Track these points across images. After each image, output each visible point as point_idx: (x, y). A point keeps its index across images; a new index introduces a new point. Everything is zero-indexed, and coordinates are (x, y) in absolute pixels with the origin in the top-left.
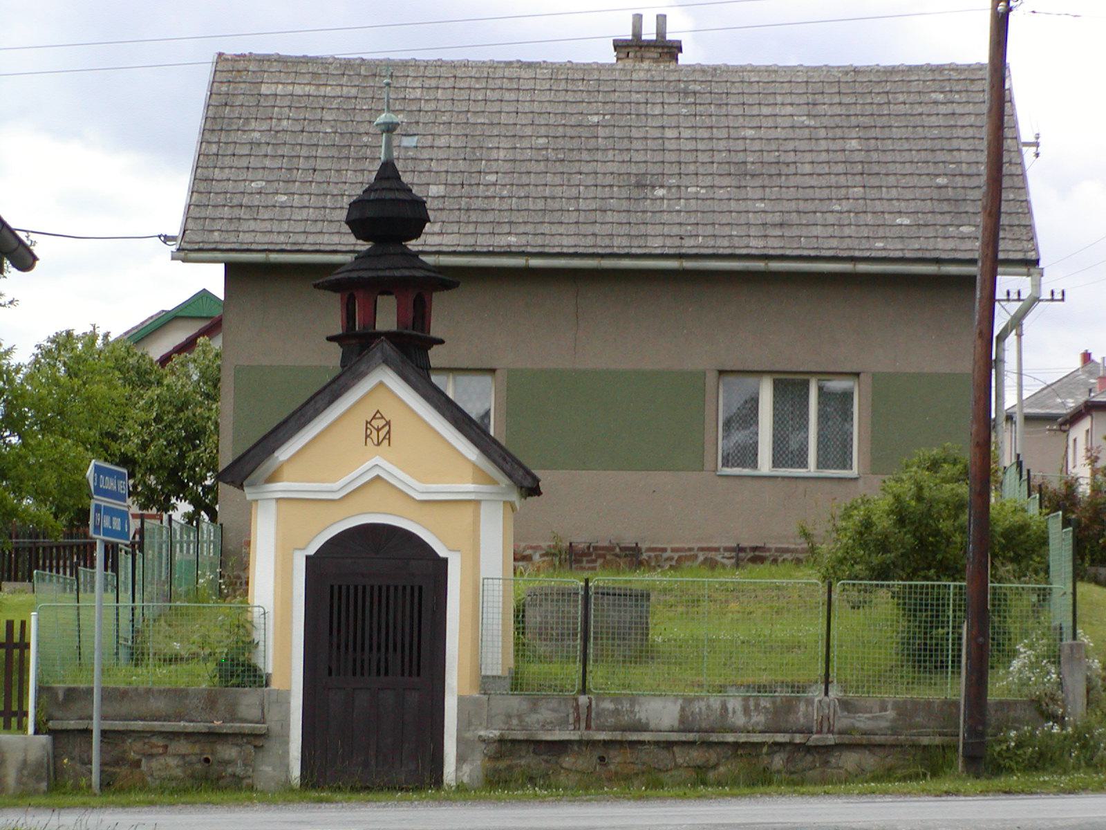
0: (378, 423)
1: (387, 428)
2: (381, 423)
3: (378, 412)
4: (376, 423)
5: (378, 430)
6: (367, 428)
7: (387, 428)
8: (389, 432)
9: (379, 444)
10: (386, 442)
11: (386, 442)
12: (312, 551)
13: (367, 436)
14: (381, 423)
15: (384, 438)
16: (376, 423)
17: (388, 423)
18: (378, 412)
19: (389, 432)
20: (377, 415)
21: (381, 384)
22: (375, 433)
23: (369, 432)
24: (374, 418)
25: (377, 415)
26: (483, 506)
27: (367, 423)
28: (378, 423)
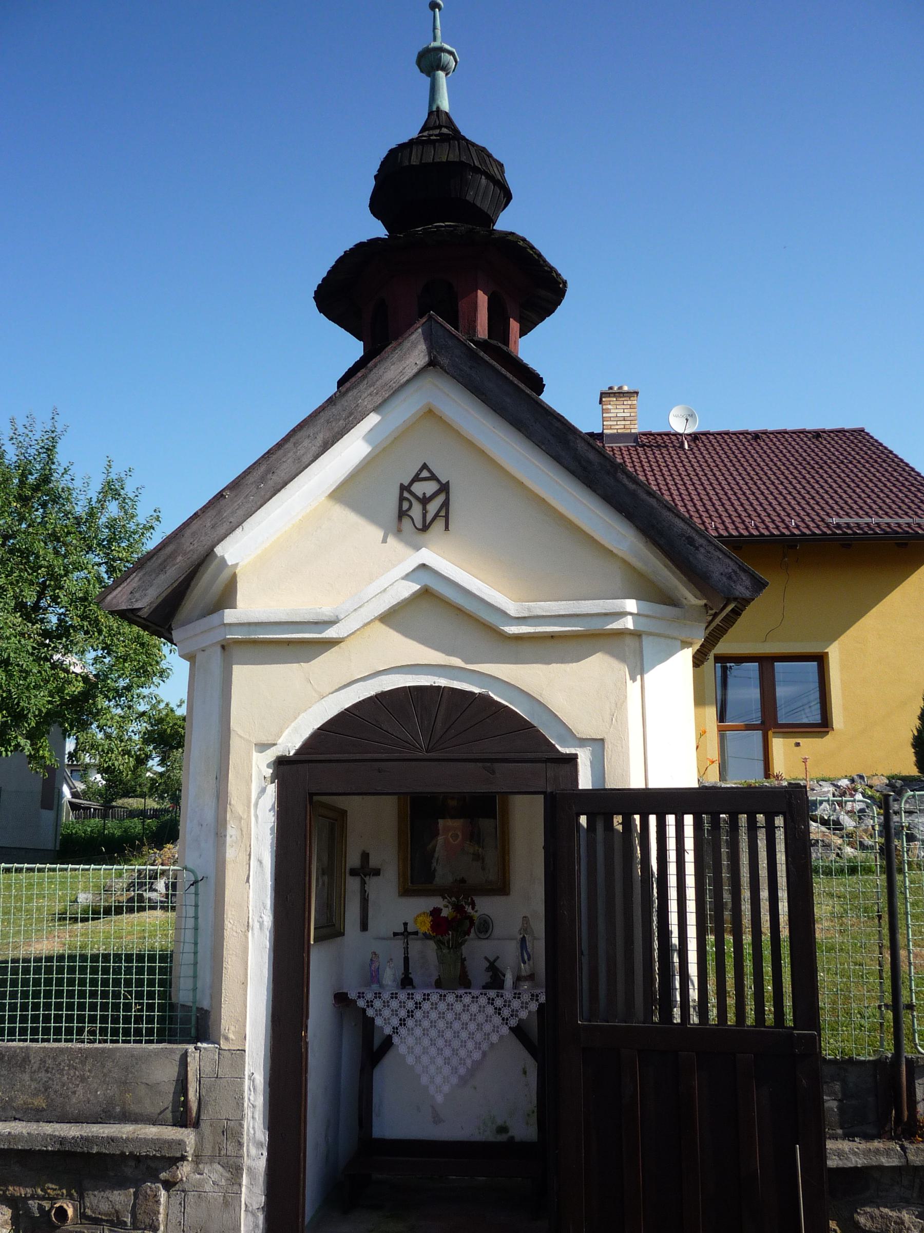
0: (425, 488)
1: (441, 499)
2: (429, 488)
3: (425, 467)
4: (420, 489)
6: (402, 499)
7: (441, 499)
8: (446, 504)
9: (425, 528)
10: (440, 523)
11: (440, 523)
12: (291, 741)
13: (402, 514)
15: (436, 516)
16: (420, 489)
17: (444, 488)
18: (425, 467)
20: (425, 473)
21: (430, 413)
23: (406, 505)
24: (417, 479)
25: (425, 473)
26: (646, 641)
27: (403, 488)
28: (425, 488)
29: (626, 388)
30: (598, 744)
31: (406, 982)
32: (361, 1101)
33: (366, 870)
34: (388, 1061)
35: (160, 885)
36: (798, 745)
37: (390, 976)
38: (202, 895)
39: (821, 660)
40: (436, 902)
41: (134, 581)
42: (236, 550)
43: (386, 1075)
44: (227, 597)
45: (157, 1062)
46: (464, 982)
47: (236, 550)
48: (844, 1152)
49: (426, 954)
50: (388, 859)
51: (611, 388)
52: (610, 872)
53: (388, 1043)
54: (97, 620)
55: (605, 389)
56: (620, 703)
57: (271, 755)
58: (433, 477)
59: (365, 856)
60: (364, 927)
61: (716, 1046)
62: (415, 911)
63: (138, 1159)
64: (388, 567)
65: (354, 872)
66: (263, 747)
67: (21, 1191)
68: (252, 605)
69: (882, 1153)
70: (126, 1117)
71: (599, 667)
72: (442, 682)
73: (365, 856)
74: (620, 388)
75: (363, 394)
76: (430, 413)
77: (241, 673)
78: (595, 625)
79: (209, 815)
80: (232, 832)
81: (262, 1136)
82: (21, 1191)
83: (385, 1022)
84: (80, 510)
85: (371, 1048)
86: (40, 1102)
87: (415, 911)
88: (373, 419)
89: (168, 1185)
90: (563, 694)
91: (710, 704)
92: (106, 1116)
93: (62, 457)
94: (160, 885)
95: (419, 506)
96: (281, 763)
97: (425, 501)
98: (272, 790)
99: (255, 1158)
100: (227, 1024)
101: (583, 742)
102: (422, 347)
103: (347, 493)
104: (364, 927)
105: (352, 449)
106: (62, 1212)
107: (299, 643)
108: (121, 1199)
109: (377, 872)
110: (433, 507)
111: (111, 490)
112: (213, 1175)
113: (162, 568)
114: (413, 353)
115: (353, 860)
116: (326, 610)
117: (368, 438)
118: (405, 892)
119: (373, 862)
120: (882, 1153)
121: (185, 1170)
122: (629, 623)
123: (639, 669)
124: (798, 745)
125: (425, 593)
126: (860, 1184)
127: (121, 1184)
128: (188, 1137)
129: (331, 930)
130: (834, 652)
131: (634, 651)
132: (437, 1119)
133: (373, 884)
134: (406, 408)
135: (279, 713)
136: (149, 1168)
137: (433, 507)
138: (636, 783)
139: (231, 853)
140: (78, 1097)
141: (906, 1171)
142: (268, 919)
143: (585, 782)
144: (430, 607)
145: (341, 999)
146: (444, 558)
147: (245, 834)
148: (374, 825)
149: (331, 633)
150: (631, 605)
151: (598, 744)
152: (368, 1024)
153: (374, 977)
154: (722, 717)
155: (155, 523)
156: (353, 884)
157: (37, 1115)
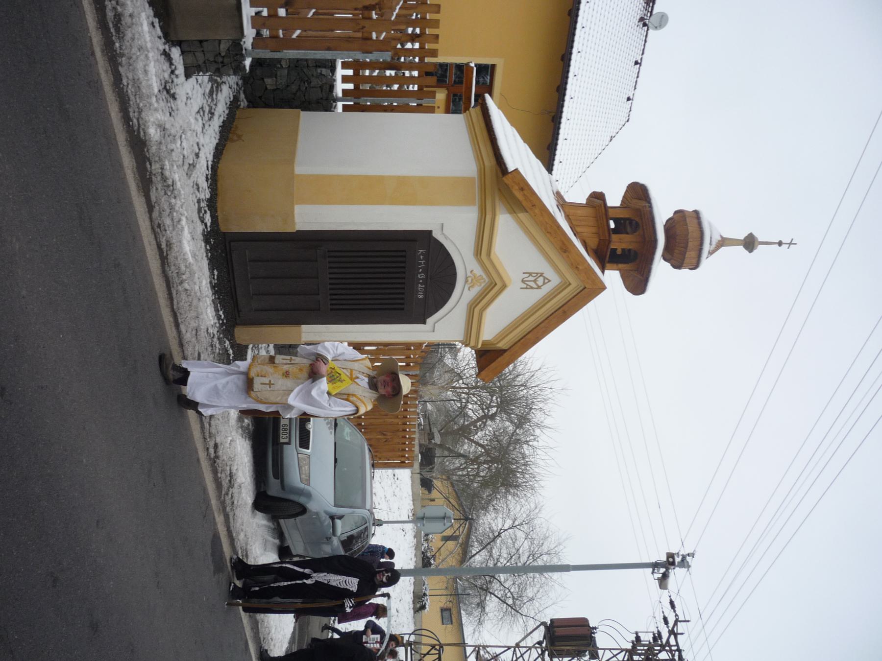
1: (535, 286)
3: (549, 281)
5: (535, 281)
7: (535, 286)
8: (532, 288)
9: (523, 281)
10: (525, 286)
11: (525, 286)
13: (530, 274)
17: (539, 287)
18: (549, 281)
19: (532, 288)
20: (547, 281)
22: (533, 279)
24: (545, 278)
25: (547, 281)
27: (541, 275)
28: (540, 281)
58: (544, 283)
97: (535, 281)
110: (532, 284)
137: (532, 284)
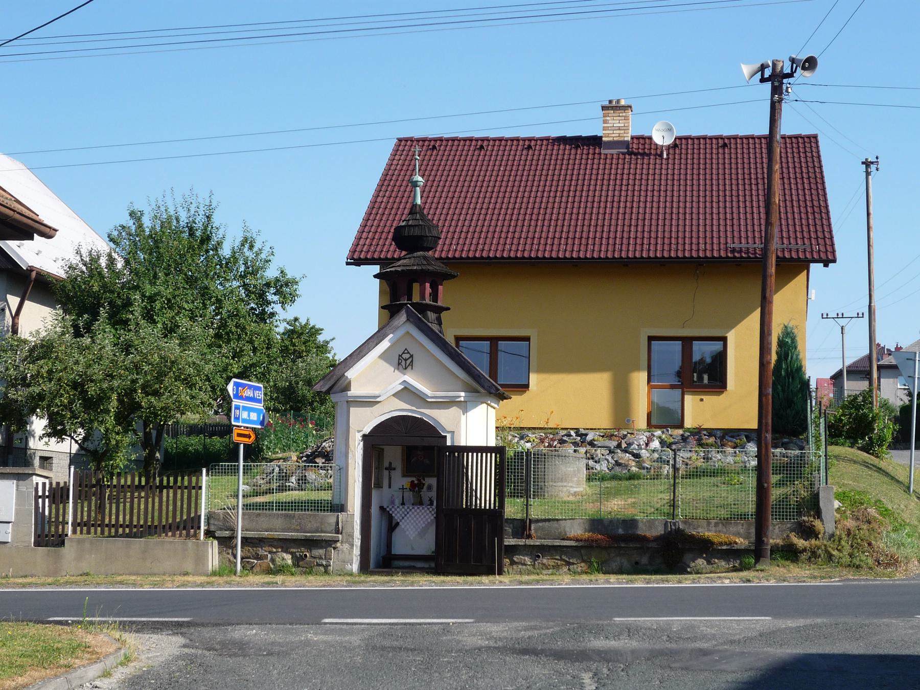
0: (406, 356)
2: (407, 356)
4: (405, 356)
5: (406, 360)
12: (367, 430)
13: (399, 364)
14: (407, 356)
16: (405, 356)
17: (412, 356)
20: (406, 351)
21: (408, 333)
22: (403, 362)
25: (406, 351)
29: (623, 103)
30: (453, 433)
31: (403, 504)
32: (389, 544)
33: (390, 468)
34: (397, 530)
35: (293, 479)
36: (702, 400)
37: (398, 501)
38: (343, 471)
39: (724, 339)
40: (414, 479)
41: (321, 383)
42: (351, 374)
43: (397, 536)
44: (347, 387)
45: (331, 518)
46: (421, 503)
47: (351, 374)
48: (509, 541)
49: (409, 495)
50: (398, 464)
51: (610, 102)
52: (454, 467)
53: (398, 524)
54: (245, 328)
55: (607, 103)
56: (459, 421)
57: (362, 433)
59: (390, 464)
60: (390, 487)
61: (481, 513)
62: (406, 482)
63: (326, 541)
64: (395, 379)
65: (386, 469)
66: (359, 431)
67: (294, 550)
68: (356, 391)
69: (521, 542)
70: (322, 532)
71: (454, 410)
72: (410, 414)
73: (390, 464)
74: (618, 101)
75: (387, 329)
76: (408, 333)
77: (353, 410)
78: (453, 399)
79: (343, 449)
80: (350, 455)
81: (359, 537)
82: (294, 550)
83: (397, 516)
84: (226, 251)
85: (392, 526)
86: (298, 527)
87: (406, 482)
88: (391, 336)
89: (334, 548)
90: (443, 418)
91: (643, 370)
92: (317, 531)
93: (216, 220)
94: (293, 479)
95: (404, 361)
96: (364, 436)
97: (406, 360)
98: (362, 443)
99: (357, 542)
100: (349, 507)
101: (449, 432)
102: (405, 315)
103: (384, 356)
104: (390, 487)
105: (385, 344)
106: (306, 556)
107: (369, 402)
108: (321, 552)
109: (394, 469)
110: (408, 362)
111: (248, 242)
112: (346, 546)
113: (330, 379)
114: (402, 317)
115: (386, 464)
116: (377, 393)
117: (389, 341)
118: (404, 476)
119: (393, 466)
120: (521, 542)
121: (339, 545)
122: (462, 399)
123: (465, 411)
124: (702, 400)
125: (405, 388)
126: (512, 550)
127: (322, 548)
128: (340, 536)
129: (379, 486)
130: (731, 336)
131: (465, 407)
132: (413, 549)
133: (393, 472)
134: (400, 333)
135: (363, 422)
136: (329, 544)
137: (408, 362)
138: (463, 444)
139: (350, 461)
140: (309, 526)
141: (525, 546)
142: (361, 480)
143: (449, 443)
144: (407, 393)
145: (382, 508)
146: (411, 379)
147: (354, 456)
148: (393, 454)
149: (378, 400)
150: (463, 394)
151: (453, 433)
152: (390, 517)
153: (393, 502)
154: (649, 381)
155: (271, 258)
156: (386, 473)
157: (298, 531)
